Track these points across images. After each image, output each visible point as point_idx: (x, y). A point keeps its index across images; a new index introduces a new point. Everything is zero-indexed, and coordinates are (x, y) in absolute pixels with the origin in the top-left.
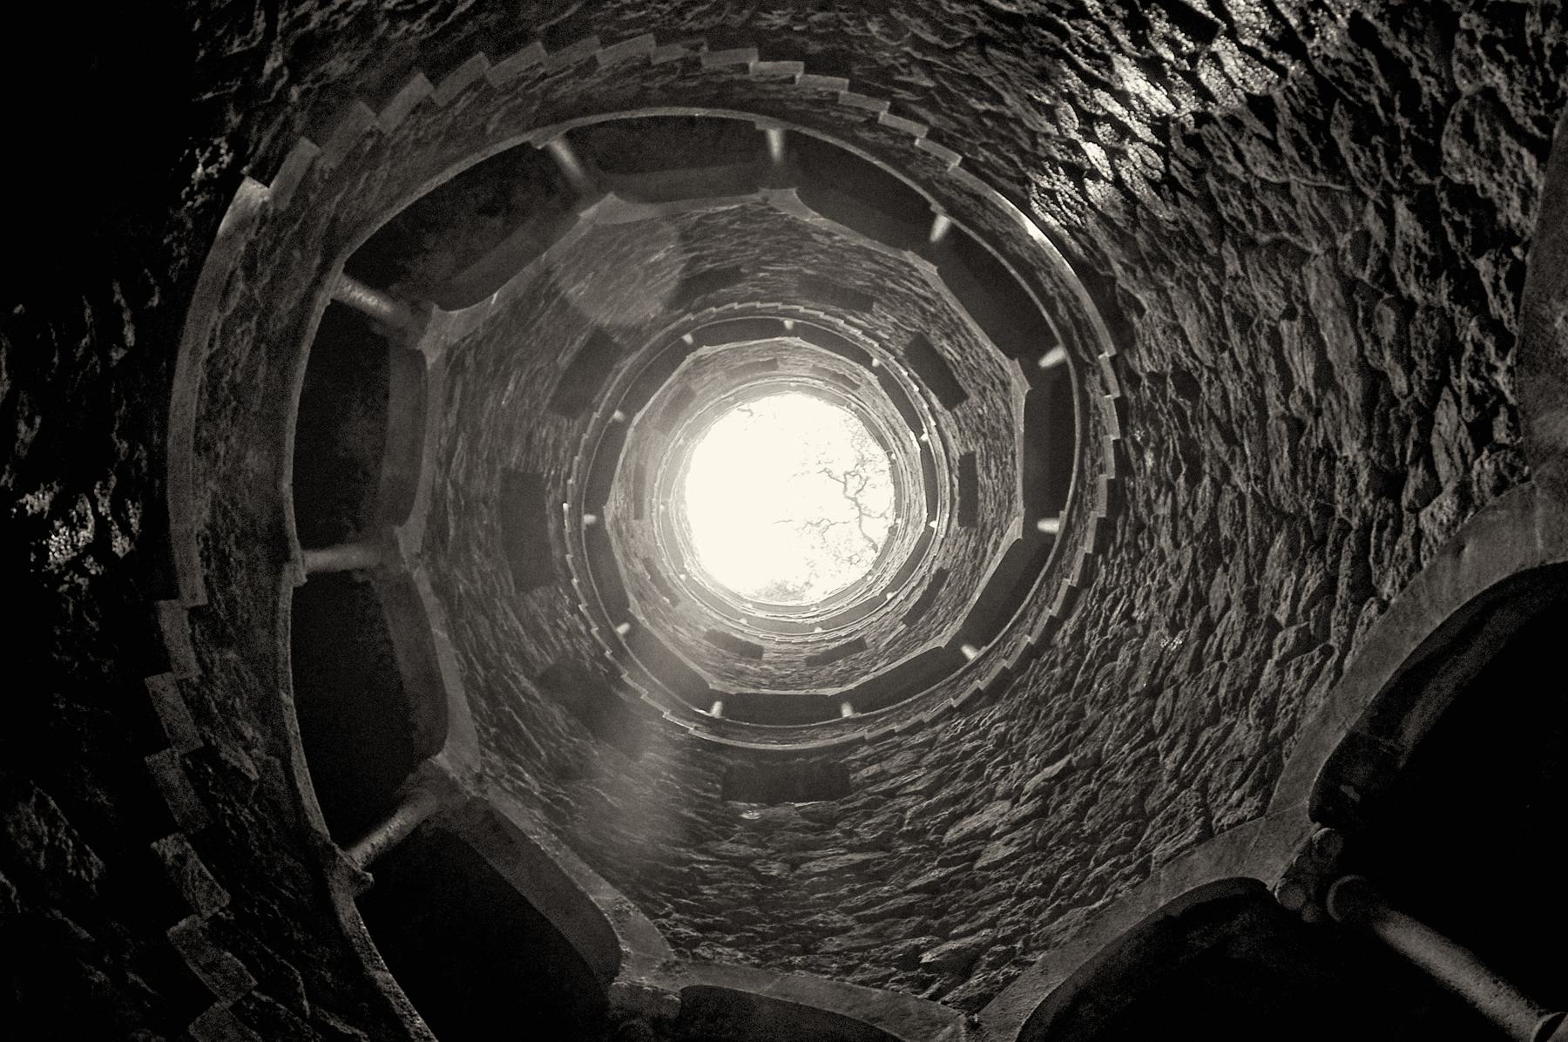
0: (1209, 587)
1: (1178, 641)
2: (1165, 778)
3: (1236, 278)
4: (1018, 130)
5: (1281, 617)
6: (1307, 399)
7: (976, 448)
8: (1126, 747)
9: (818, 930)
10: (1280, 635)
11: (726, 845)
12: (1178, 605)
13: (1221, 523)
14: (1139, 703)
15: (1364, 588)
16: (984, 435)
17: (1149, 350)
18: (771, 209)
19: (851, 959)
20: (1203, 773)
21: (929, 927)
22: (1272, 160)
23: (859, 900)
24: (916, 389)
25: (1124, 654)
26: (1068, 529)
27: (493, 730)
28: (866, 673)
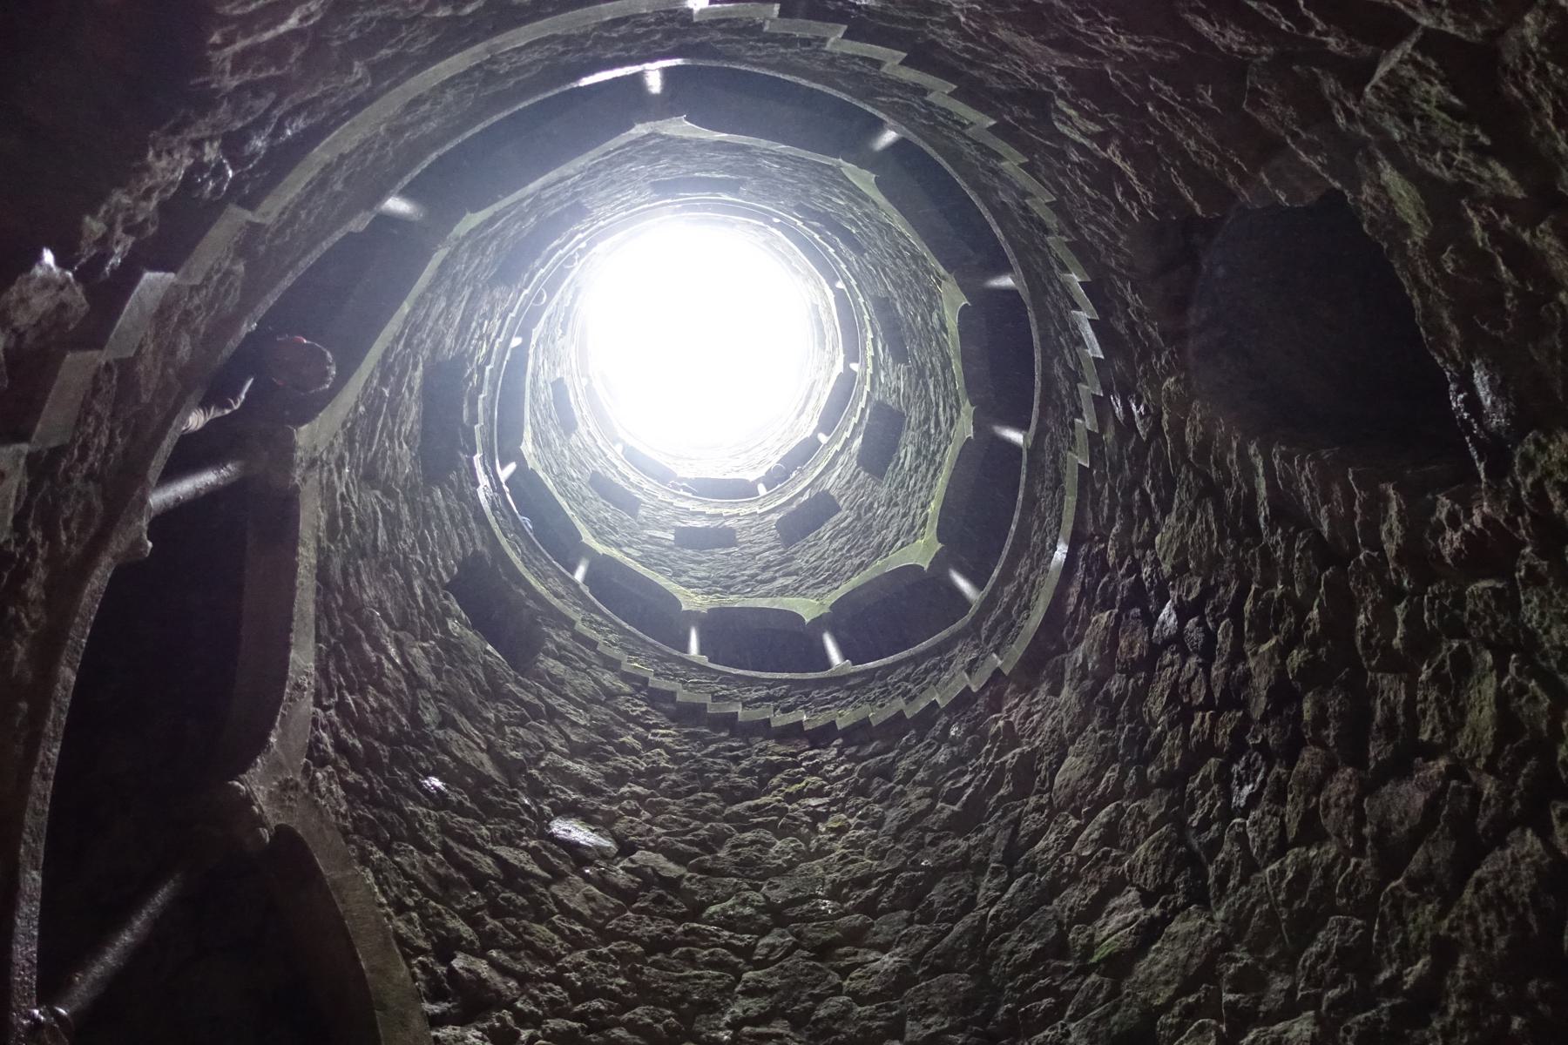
0: (884, 911)
1: (827, 905)
2: (727, 1018)
3: (1143, 816)
4: (1146, 528)
7: (845, 516)
9: (411, 828)
13: (939, 887)
16: (859, 518)
17: (1028, 715)
18: (940, 284)
19: (411, 895)
22: (1271, 846)
24: (855, 420)
26: (840, 680)
27: (362, 409)
28: (618, 546)
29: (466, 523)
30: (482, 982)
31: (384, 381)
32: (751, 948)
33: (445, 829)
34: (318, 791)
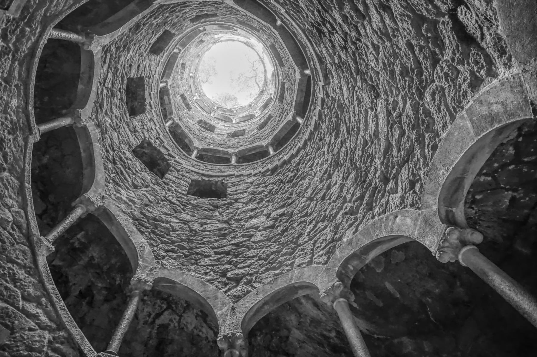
0: (333, 174)
2: (306, 234)
5: (348, 197)
6: (370, 136)
8: (299, 215)
9: (201, 254)
10: (346, 204)
11: (183, 215)
12: (325, 173)
14: (306, 201)
15: (370, 207)
20: (315, 239)
21: (232, 261)
23: (216, 244)
25: (307, 180)
27: (112, 175)
29: (183, 176)
30: (237, 274)
31: (114, 163)
32: (307, 213)
33: (213, 248)
34: (165, 265)
